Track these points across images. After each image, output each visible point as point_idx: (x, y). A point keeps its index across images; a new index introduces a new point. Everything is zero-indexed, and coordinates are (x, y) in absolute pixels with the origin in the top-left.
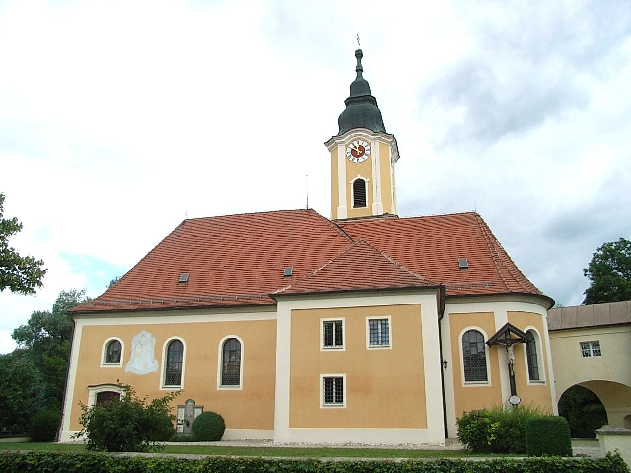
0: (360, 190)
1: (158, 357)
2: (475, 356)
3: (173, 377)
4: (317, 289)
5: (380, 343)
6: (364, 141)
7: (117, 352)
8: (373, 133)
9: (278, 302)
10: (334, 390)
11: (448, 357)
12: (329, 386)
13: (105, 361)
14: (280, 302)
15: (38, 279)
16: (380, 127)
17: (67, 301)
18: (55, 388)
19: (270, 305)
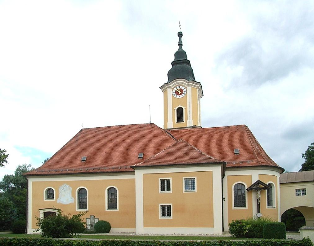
0: (180, 113)
1: (73, 196)
2: (240, 195)
3: (82, 205)
4: (157, 164)
5: (190, 189)
6: (183, 86)
7: (52, 194)
8: (188, 81)
9: (136, 170)
10: (166, 211)
11: (226, 196)
12: (163, 209)
13: (46, 198)
14: (137, 170)
15: (5, 159)
16: (192, 78)
17: (22, 170)
18: (22, 210)
19: (131, 172)
